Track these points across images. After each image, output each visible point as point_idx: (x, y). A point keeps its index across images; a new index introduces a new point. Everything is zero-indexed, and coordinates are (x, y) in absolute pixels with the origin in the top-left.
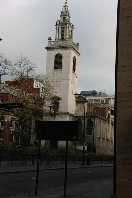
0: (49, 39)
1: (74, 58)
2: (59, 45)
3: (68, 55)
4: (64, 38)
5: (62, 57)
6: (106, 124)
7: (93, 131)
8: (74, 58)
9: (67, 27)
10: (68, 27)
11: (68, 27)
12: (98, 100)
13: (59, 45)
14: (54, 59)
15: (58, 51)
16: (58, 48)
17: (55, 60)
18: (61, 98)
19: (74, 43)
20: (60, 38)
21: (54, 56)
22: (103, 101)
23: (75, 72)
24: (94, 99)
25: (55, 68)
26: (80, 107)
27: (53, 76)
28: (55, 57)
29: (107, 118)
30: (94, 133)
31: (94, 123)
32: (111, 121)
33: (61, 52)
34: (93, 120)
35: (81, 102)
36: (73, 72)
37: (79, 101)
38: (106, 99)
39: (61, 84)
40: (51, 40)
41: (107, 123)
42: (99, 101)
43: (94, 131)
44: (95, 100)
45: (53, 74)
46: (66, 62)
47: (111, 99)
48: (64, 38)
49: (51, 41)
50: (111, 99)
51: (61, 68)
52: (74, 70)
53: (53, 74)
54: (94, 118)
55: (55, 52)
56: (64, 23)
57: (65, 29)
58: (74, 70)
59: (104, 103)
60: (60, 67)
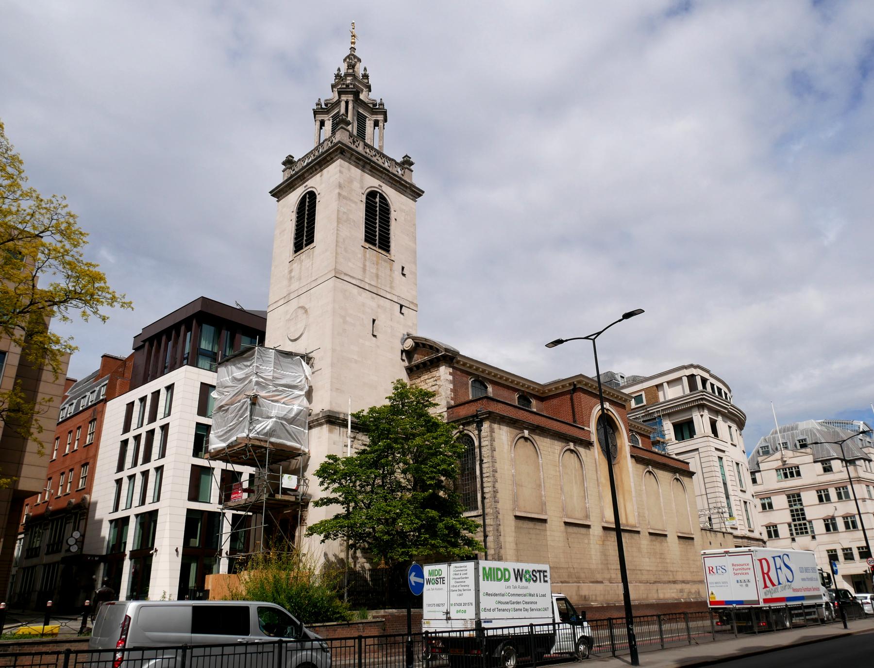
0: (284, 163)
7: (479, 486)
23: (388, 251)
30: (483, 498)
31: (480, 447)
34: (473, 433)
36: (367, 245)
37: (418, 367)
41: (594, 456)
43: (482, 488)
45: (291, 271)
47: (665, 385)
50: (665, 385)
53: (291, 271)
59: (645, 403)
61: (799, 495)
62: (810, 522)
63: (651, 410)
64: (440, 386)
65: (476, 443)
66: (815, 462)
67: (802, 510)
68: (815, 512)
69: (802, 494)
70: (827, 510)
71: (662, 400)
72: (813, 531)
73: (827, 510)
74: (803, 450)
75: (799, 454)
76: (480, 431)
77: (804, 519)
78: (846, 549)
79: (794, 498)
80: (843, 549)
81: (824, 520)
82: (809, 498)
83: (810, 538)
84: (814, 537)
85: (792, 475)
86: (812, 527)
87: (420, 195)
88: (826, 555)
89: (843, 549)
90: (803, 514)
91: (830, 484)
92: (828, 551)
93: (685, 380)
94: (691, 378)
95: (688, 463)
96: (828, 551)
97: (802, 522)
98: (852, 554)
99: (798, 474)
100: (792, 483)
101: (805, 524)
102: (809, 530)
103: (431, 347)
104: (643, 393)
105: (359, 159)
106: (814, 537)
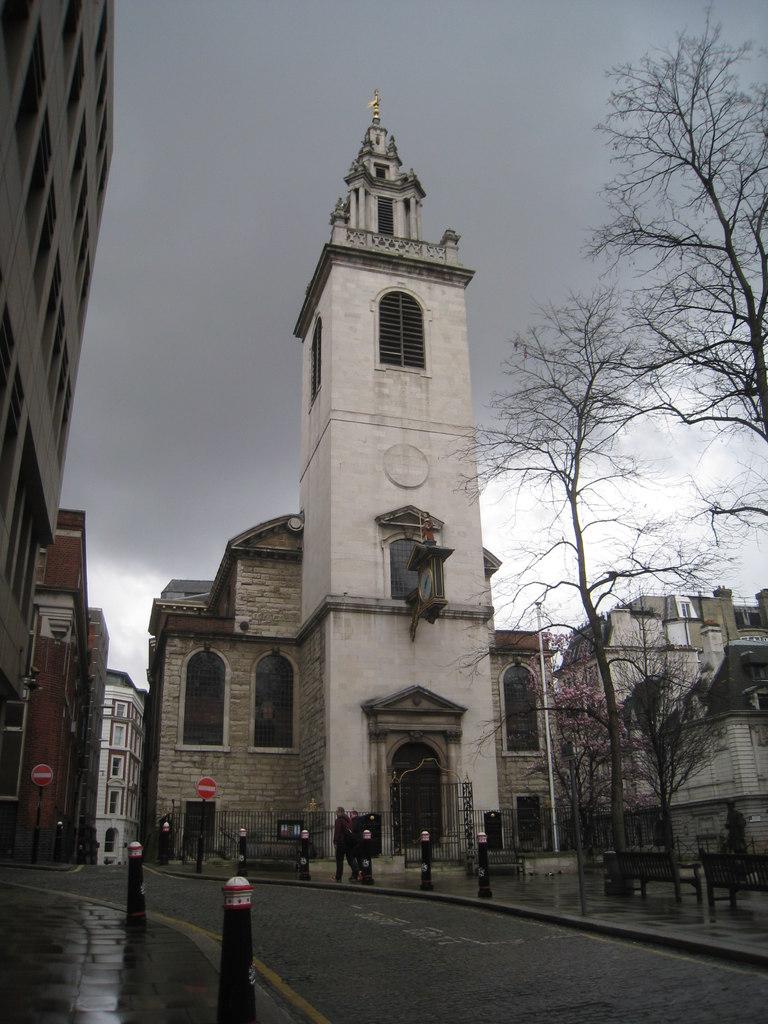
15: (400, 279)
21: (378, 299)
27: (381, 395)
33: (418, 288)
39: (430, 447)
46: (447, 338)
53: (381, 385)
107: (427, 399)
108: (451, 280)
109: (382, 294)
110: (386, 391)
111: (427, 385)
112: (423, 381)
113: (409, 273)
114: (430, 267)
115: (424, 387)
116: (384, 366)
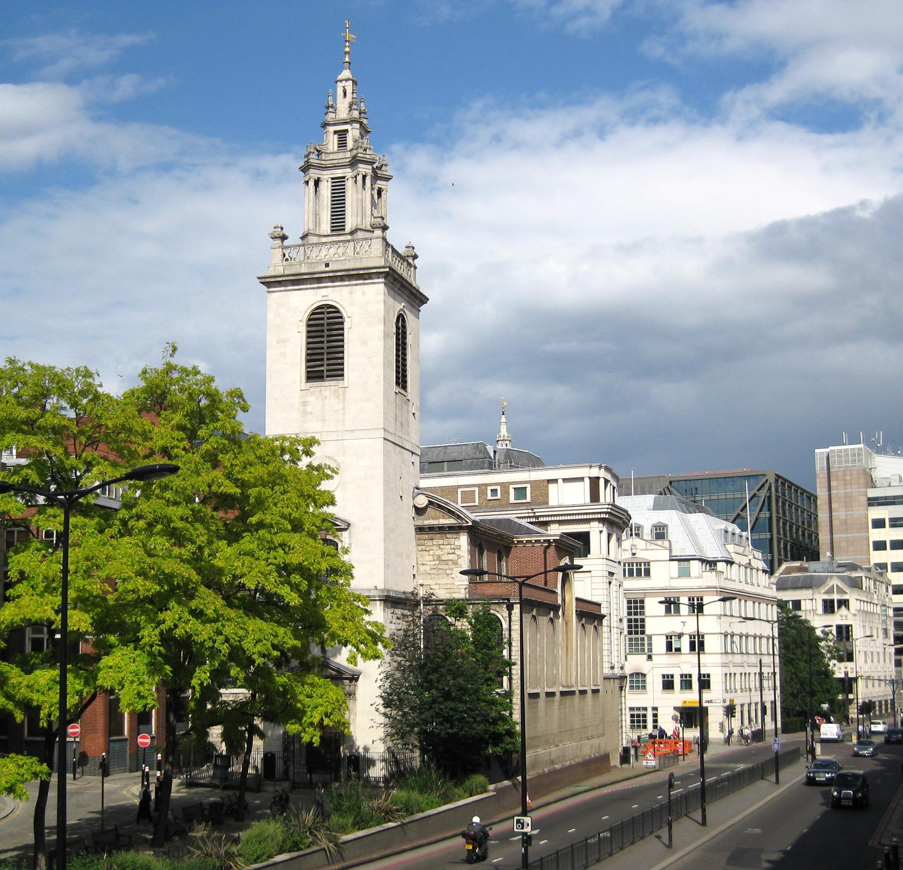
1: (401, 318)
2: (327, 265)
3: (366, 310)
4: (348, 230)
5: (342, 323)
6: (556, 625)
8: (401, 318)
9: (360, 178)
10: (364, 177)
11: (364, 177)
12: (499, 488)
13: (327, 265)
14: (303, 329)
15: (324, 292)
16: (319, 280)
17: (310, 334)
18: (349, 525)
19: (394, 251)
20: (326, 227)
21: (305, 318)
22: (520, 492)
23: (404, 387)
24: (479, 486)
25: (313, 376)
26: (439, 558)
27: (305, 413)
28: (309, 320)
29: (559, 590)
32: (577, 599)
35: (441, 530)
37: (431, 529)
38: (535, 484)
40: (284, 238)
42: (506, 492)
44: (482, 487)
45: (305, 404)
46: (364, 343)
47: (560, 481)
48: (348, 230)
49: (286, 243)
50: (560, 481)
51: (342, 375)
52: (401, 380)
53: (305, 404)
54: (510, 608)
55: (307, 299)
56: (341, 155)
57: (349, 184)
58: (401, 380)
60: (337, 372)
61: (642, 602)
62: (650, 638)
63: (539, 511)
64: (459, 557)
65: (505, 625)
66: (671, 560)
67: (643, 620)
68: (658, 623)
69: (647, 600)
70: (673, 624)
71: (552, 501)
72: (650, 650)
73: (673, 624)
74: (660, 542)
75: (653, 547)
76: (510, 615)
77: (643, 633)
78: (686, 676)
79: (636, 606)
80: (682, 676)
81: (667, 638)
82: (654, 607)
83: (645, 657)
84: (650, 657)
85: (639, 573)
86: (650, 644)
87: (424, 303)
88: (660, 680)
89: (682, 676)
90: (643, 626)
91: (684, 591)
92: (664, 676)
93: (587, 481)
94: (594, 481)
95: (599, 605)
96: (664, 676)
97: (639, 636)
98: (690, 682)
99: (648, 573)
100: (636, 584)
101: (643, 639)
102: (646, 647)
103: (449, 511)
104: (528, 486)
105: (395, 280)
106: (650, 657)
107: (344, 408)
108: (371, 278)
109: (309, 311)
110: (309, 409)
111: (344, 393)
112: (341, 391)
113: (333, 282)
114: (347, 273)
115: (341, 397)
116: (309, 384)
